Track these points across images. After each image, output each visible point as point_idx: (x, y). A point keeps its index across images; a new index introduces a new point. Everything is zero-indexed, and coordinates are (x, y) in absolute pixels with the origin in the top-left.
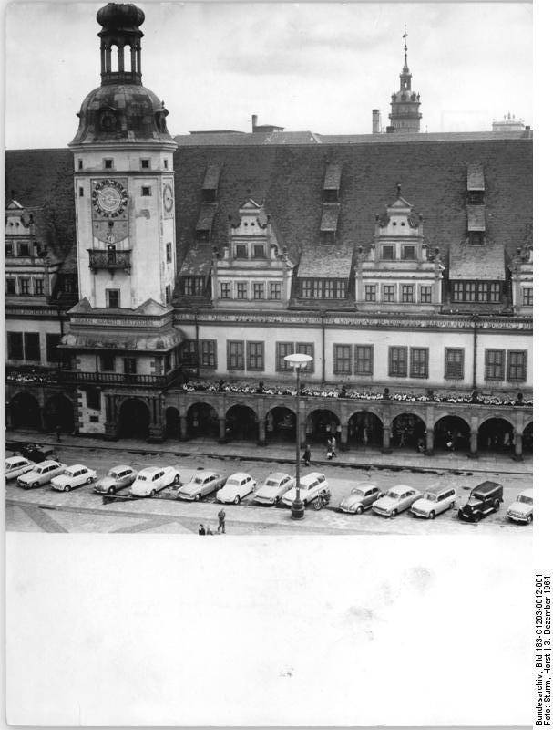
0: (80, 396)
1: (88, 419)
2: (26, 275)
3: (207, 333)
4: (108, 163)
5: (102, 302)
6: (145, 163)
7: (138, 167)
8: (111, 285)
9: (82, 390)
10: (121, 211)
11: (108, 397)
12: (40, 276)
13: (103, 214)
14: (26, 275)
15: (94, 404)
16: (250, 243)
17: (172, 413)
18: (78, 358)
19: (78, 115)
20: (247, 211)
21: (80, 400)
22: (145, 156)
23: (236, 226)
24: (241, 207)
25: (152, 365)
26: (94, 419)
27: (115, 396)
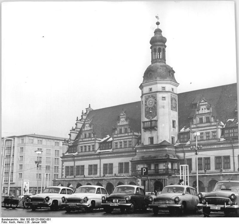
0: (139, 181)
2: (126, 140)
4: (151, 89)
5: (147, 142)
6: (164, 88)
7: (160, 89)
8: (150, 136)
10: (154, 106)
12: (130, 140)
13: (148, 108)
14: (126, 140)
16: (204, 117)
19: (143, 77)
20: (202, 104)
21: (139, 183)
27: (151, 179)
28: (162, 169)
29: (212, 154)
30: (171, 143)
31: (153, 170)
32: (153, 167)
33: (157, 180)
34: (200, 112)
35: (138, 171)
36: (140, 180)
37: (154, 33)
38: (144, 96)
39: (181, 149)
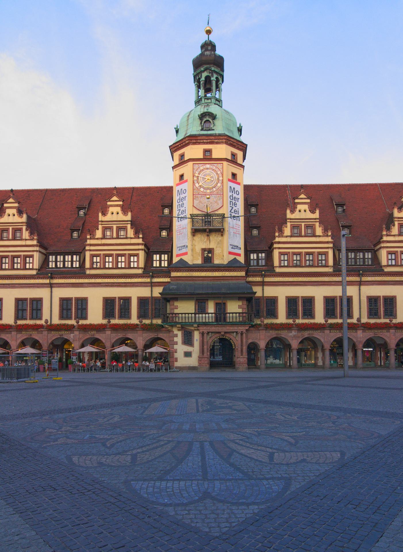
0: (176, 336)
1: (182, 355)
3: (270, 292)
9: (179, 330)
11: (202, 334)
15: (188, 340)
17: (253, 348)
18: (176, 303)
21: (176, 339)
22: (235, 151)
23: (292, 212)
24: (297, 198)
25: (240, 307)
26: (188, 354)
27: (208, 333)
28: (236, 313)
29: (319, 294)
30: (243, 262)
31: (212, 313)
32: (211, 308)
33: (223, 333)
34: (296, 215)
35: (176, 314)
36: (180, 334)
37: (202, 47)
38: (190, 164)
39: (259, 279)
